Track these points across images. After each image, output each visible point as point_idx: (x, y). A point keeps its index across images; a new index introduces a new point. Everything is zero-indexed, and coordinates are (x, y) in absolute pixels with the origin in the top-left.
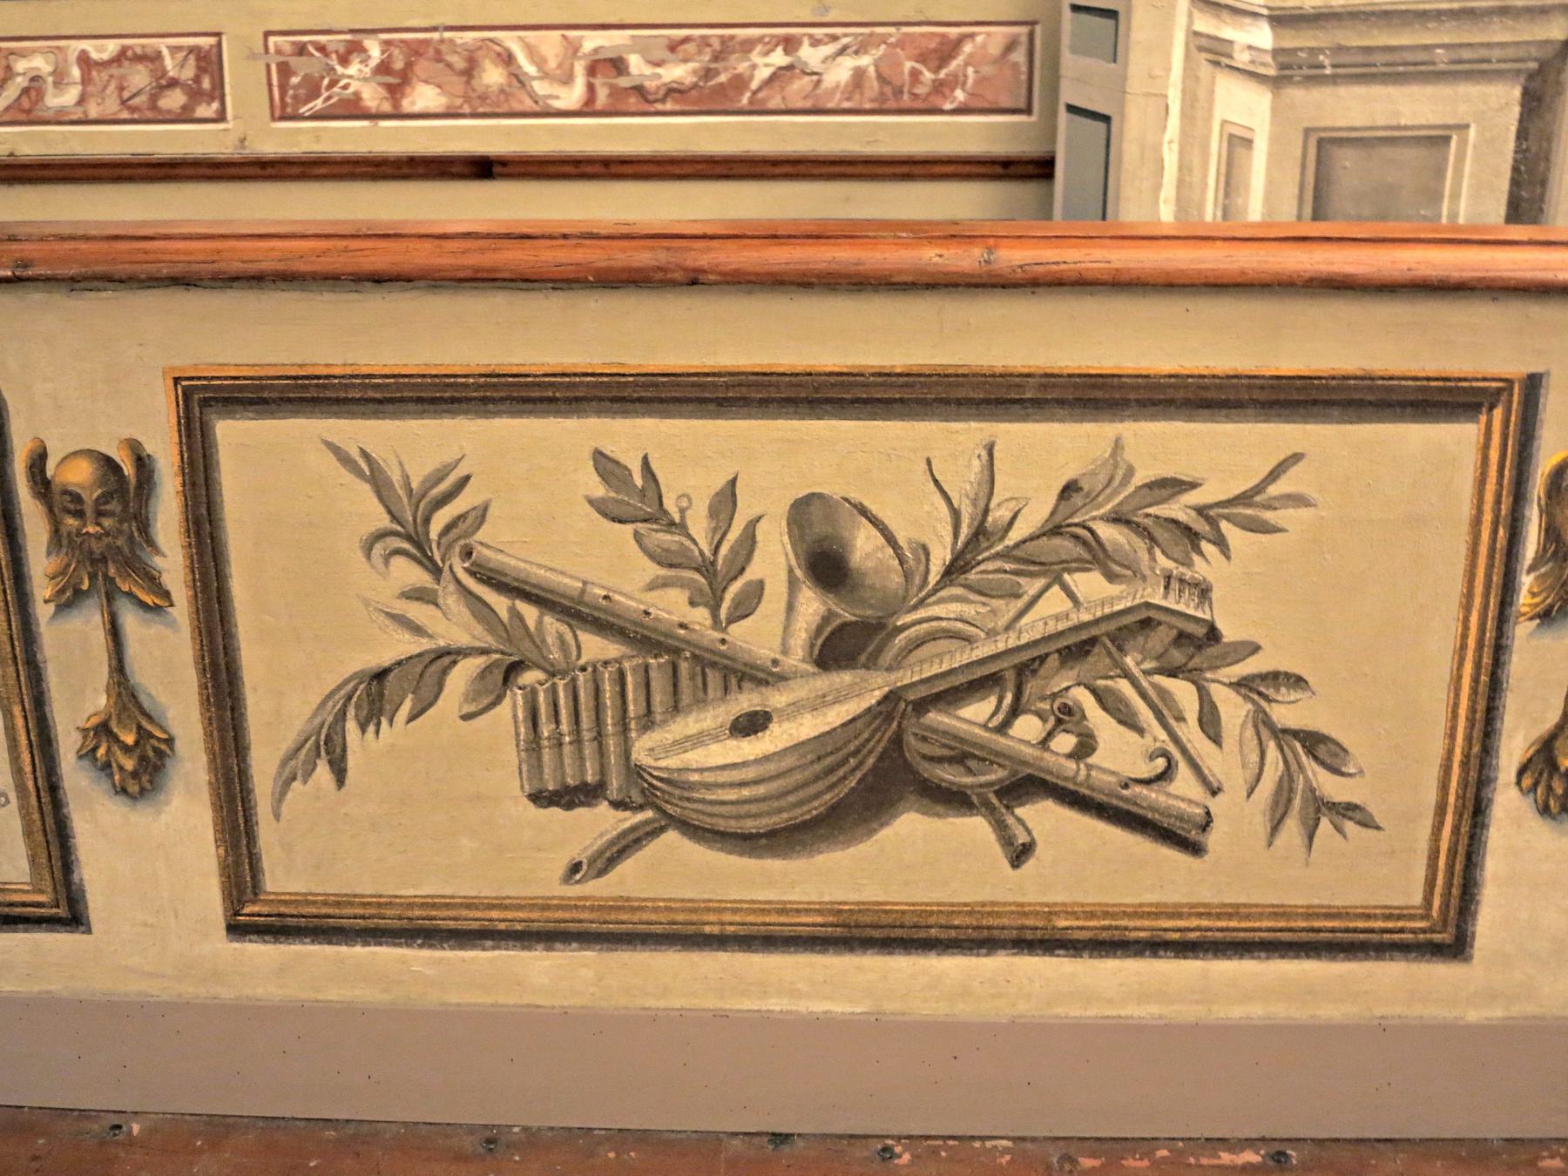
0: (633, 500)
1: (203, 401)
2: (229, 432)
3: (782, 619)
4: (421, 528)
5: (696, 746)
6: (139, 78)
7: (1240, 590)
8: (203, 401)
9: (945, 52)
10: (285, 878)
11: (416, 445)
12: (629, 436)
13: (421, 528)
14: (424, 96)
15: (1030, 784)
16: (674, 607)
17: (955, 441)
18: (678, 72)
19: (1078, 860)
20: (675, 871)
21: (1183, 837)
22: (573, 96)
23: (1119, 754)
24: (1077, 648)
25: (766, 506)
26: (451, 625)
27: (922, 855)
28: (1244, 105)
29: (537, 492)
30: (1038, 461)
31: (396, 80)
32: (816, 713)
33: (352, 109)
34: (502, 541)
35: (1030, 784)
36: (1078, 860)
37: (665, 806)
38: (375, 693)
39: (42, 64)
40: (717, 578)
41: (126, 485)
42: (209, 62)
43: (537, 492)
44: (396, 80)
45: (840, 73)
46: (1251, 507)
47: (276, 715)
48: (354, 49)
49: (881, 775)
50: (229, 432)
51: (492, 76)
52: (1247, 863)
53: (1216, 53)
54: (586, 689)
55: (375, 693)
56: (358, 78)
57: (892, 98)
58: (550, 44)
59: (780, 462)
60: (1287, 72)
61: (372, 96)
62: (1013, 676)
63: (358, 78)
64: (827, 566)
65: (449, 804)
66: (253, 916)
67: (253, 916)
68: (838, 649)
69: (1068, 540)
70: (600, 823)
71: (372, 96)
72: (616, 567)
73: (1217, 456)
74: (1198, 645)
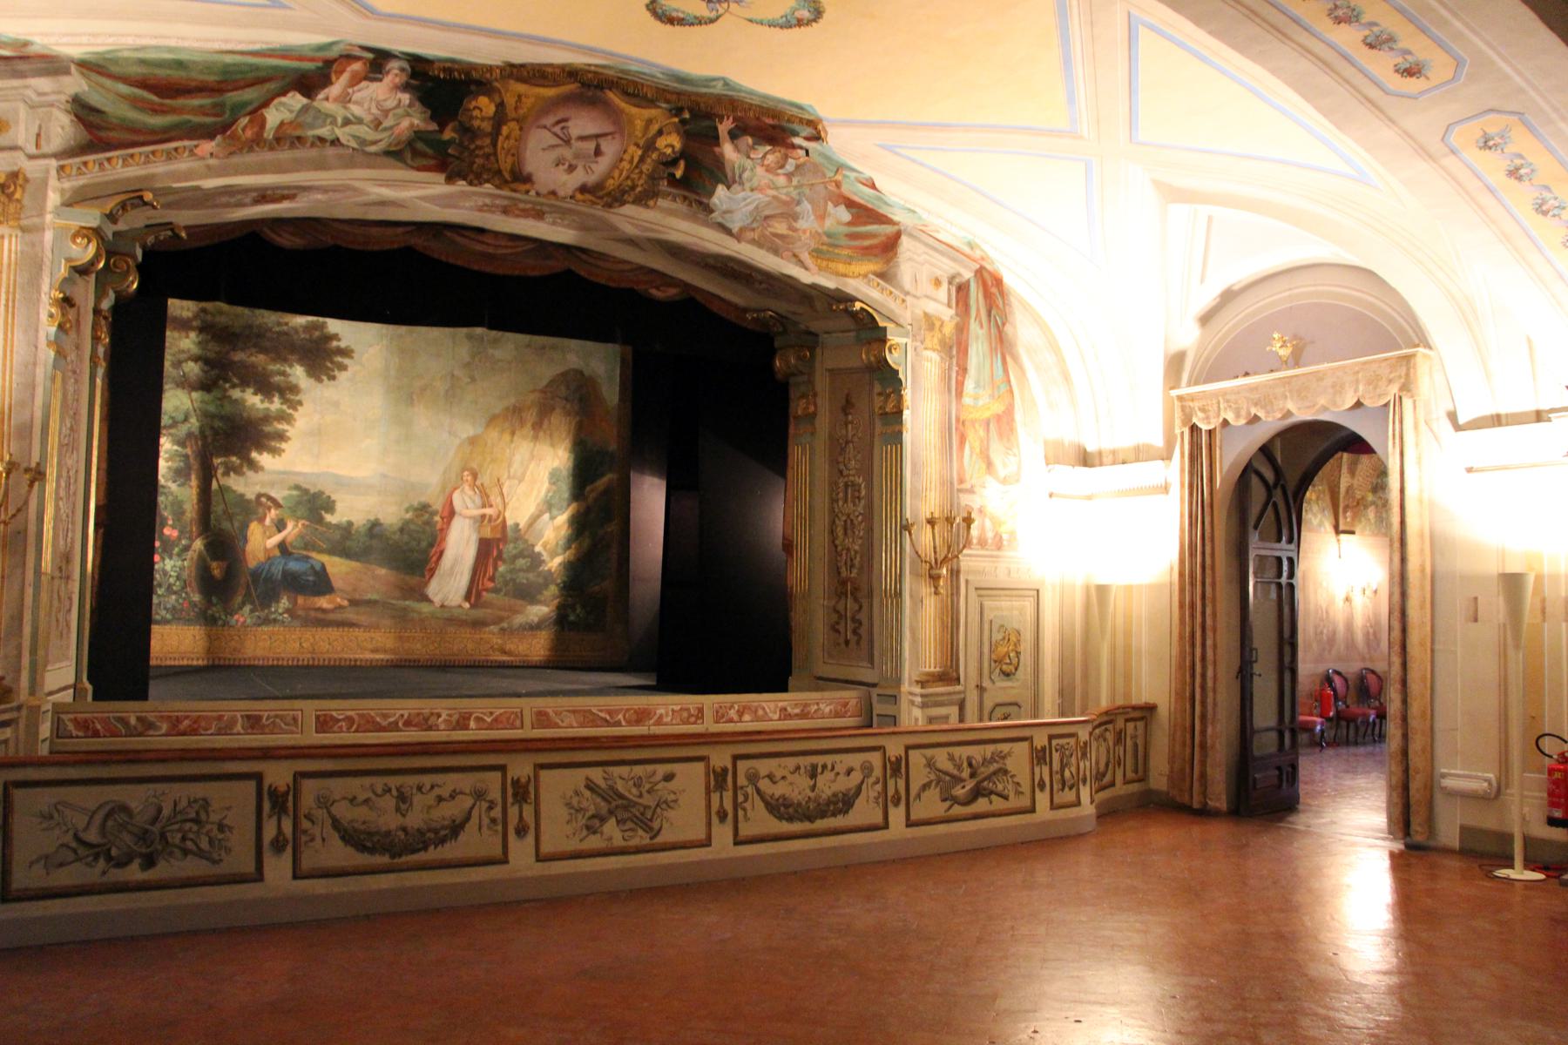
0: (951, 758)
1: (908, 748)
2: (911, 752)
3: (966, 774)
4: (930, 764)
5: (959, 792)
6: (685, 714)
7: (1010, 764)
8: (908, 748)
9: (846, 705)
10: (913, 817)
11: (929, 752)
12: (951, 749)
13: (930, 764)
14: (747, 717)
15: (992, 792)
16: (955, 772)
17: (981, 748)
18: (797, 711)
19: (998, 804)
20: (958, 810)
21: (1006, 798)
22: (776, 716)
23: (1000, 787)
24: (994, 773)
25: (964, 757)
26: (933, 777)
27: (981, 805)
28: (917, 713)
29: (941, 757)
30: (990, 749)
31: (740, 714)
32: (970, 785)
33: (731, 721)
34: (940, 765)
35: (992, 792)
36: (998, 804)
37: (956, 801)
38: (925, 787)
39: (662, 711)
40: (959, 767)
41: (899, 760)
42: (701, 710)
43: (941, 757)
44: (740, 714)
45: (827, 710)
46: (1009, 754)
47: (913, 792)
48: (731, 707)
49: (977, 793)
50: (911, 752)
51: (760, 712)
52: (1014, 802)
53: (912, 703)
54: (945, 782)
55: (925, 787)
56: (733, 714)
57: (837, 715)
58: (772, 705)
59: (962, 752)
60: (924, 706)
61: (736, 718)
62: (988, 778)
63: (733, 714)
64: (970, 765)
65: (930, 805)
66: (910, 824)
67: (910, 824)
68: (972, 775)
69: (992, 760)
70: (948, 803)
71: (736, 718)
72: (948, 766)
73: (1005, 747)
74: (1006, 772)
